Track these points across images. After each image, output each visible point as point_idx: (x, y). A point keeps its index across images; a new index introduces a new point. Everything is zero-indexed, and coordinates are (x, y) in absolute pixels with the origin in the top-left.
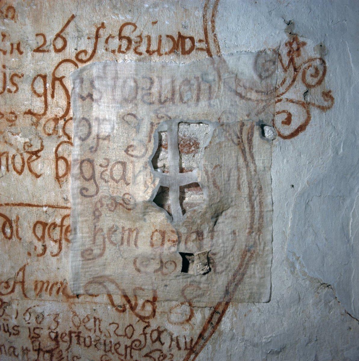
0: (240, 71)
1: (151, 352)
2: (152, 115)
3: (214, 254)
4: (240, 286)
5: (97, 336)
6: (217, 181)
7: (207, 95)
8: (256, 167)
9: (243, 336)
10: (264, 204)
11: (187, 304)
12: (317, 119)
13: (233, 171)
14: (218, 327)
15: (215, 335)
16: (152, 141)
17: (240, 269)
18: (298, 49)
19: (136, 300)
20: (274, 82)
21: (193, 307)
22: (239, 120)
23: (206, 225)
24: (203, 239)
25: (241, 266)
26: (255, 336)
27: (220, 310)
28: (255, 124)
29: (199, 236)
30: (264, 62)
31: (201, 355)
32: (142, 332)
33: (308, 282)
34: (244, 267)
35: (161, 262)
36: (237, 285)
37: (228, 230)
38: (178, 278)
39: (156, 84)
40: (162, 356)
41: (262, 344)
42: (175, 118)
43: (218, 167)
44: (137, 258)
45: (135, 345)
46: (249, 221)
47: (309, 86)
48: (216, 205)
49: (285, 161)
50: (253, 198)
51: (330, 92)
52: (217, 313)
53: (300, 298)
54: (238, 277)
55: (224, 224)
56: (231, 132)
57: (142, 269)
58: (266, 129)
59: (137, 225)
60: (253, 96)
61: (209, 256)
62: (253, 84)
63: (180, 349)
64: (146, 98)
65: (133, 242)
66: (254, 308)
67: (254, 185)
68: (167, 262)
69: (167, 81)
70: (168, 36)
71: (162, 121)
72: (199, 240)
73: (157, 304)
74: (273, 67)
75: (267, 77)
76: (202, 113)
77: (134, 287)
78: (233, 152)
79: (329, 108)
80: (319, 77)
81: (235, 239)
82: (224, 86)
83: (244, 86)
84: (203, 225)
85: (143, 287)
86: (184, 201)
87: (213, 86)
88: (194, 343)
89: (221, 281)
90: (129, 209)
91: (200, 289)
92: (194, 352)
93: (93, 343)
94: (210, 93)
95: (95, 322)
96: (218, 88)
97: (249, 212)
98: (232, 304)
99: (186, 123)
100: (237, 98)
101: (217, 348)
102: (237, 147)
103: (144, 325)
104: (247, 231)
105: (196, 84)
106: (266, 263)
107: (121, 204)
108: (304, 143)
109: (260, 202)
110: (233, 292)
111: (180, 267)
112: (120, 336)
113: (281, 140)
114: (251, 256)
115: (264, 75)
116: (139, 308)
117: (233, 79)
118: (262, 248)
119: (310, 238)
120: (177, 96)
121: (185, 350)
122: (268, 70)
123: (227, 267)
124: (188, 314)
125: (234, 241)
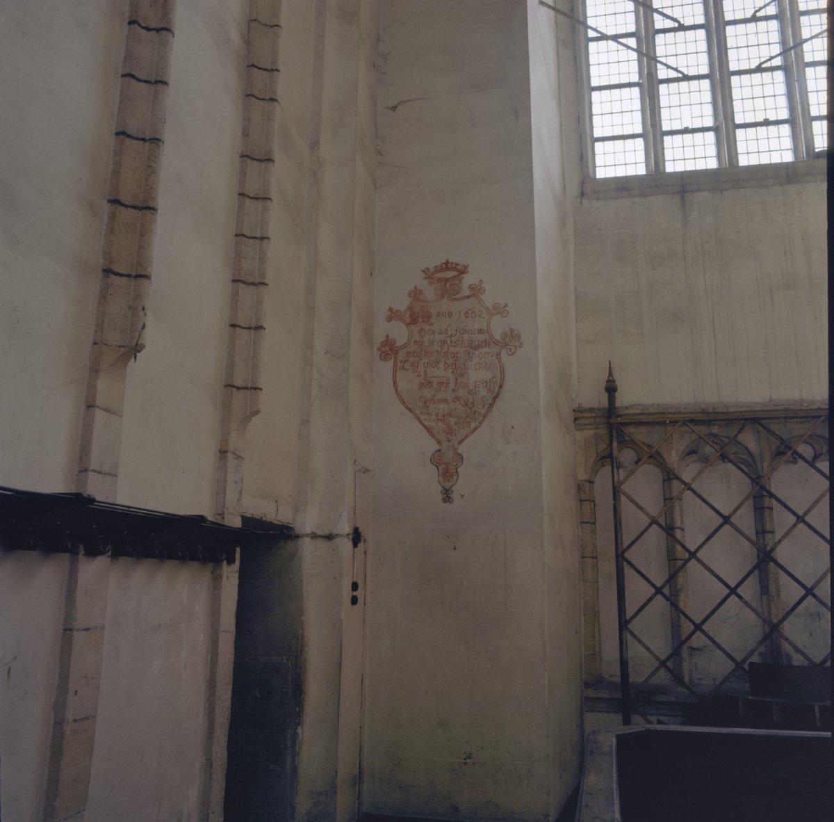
69: (477, 342)
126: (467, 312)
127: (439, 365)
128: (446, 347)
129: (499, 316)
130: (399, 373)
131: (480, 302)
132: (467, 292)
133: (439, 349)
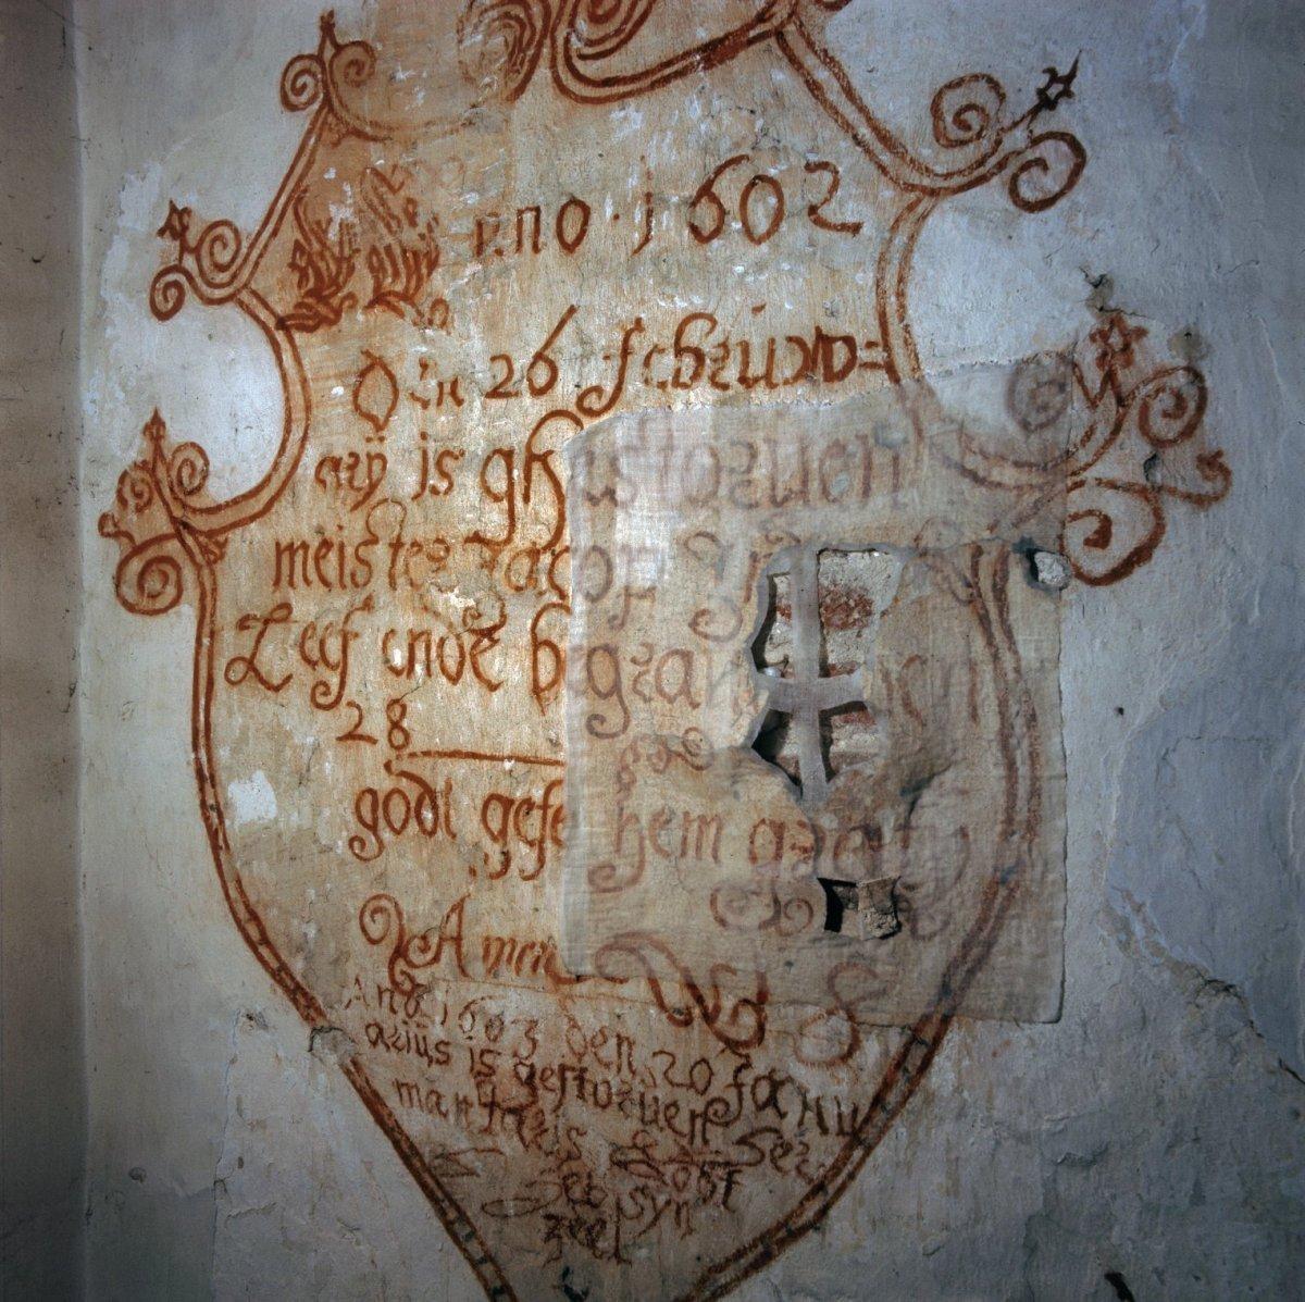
1: (752, 1134)
3: (911, 888)
4: (979, 975)
6: (915, 697)
7: (888, 480)
8: (1018, 660)
10: (1042, 759)
11: (842, 1013)
14: (923, 1081)
15: (916, 1101)
16: (754, 599)
18: (1126, 348)
19: (717, 996)
20: (1062, 437)
21: (859, 1024)
22: (967, 541)
24: (880, 846)
26: (1021, 1113)
27: (928, 1034)
29: (870, 840)
30: (1037, 387)
31: (879, 1151)
32: (730, 1080)
33: (1167, 975)
35: (776, 901)
36: (971, 972)
37: (947, 826)
38: (817, 945)
39: (763, 457)
42: (810, 541)
44: (717, 890)
45: (715, 1114)
46: (1002, 800)
47: (1158, 443)
49: (1098, 642)
50: (1013, 741)
52: (922, 1042)
53: (1144, 1020)
54: (976, 951)
55: (938, 811)
56: (948, 570)
57: (730, 918)
59: (719, 807)
60: (1008, 475)
61: (897, 892)
63: (825, 1131)
65: (709, 851)
66: (1019, 1036)
67: (1014, 709)
68: (790, 902)
69: (788, 449)
70: (790, 339)
71: (777, 549)
72: (872, 848)
73: (768, 1009)
74: (1059, 398)
75: (1042, 426)
76: (876, 525)
77: (710, 963)
79: (1216, 498)
80: (1186, 418)
82: (931, 454)
85: (733, 965)
86: (833, 749)
88: (860, 1119)
89: (931, 958)
90: (699, 768)
91: (875, 976)
92: (861, 1143)
93: (615, 1099)
94: (896, 474)
95: (619, 1045)
96: (916, 461)
98: (959, 1022)
99: (835, 551)
101: (921, 1135)
102: (966, 611)
104: (999, 828)
106: (1050, 917)
107: (680, 755)
109: (1031, 754)
111: (820, 918)
112: (678, 1085)
114: (1010, 898)
116: (724, 1017)
117: (954, 436)
120: (815, 486)
123: (946, 924)
124: (846, 1040)
126: (706, 191)
127: (495, 663)
128: (543, 504)
129: (992, 195)
131: (814, 87)
133: (493, 520)
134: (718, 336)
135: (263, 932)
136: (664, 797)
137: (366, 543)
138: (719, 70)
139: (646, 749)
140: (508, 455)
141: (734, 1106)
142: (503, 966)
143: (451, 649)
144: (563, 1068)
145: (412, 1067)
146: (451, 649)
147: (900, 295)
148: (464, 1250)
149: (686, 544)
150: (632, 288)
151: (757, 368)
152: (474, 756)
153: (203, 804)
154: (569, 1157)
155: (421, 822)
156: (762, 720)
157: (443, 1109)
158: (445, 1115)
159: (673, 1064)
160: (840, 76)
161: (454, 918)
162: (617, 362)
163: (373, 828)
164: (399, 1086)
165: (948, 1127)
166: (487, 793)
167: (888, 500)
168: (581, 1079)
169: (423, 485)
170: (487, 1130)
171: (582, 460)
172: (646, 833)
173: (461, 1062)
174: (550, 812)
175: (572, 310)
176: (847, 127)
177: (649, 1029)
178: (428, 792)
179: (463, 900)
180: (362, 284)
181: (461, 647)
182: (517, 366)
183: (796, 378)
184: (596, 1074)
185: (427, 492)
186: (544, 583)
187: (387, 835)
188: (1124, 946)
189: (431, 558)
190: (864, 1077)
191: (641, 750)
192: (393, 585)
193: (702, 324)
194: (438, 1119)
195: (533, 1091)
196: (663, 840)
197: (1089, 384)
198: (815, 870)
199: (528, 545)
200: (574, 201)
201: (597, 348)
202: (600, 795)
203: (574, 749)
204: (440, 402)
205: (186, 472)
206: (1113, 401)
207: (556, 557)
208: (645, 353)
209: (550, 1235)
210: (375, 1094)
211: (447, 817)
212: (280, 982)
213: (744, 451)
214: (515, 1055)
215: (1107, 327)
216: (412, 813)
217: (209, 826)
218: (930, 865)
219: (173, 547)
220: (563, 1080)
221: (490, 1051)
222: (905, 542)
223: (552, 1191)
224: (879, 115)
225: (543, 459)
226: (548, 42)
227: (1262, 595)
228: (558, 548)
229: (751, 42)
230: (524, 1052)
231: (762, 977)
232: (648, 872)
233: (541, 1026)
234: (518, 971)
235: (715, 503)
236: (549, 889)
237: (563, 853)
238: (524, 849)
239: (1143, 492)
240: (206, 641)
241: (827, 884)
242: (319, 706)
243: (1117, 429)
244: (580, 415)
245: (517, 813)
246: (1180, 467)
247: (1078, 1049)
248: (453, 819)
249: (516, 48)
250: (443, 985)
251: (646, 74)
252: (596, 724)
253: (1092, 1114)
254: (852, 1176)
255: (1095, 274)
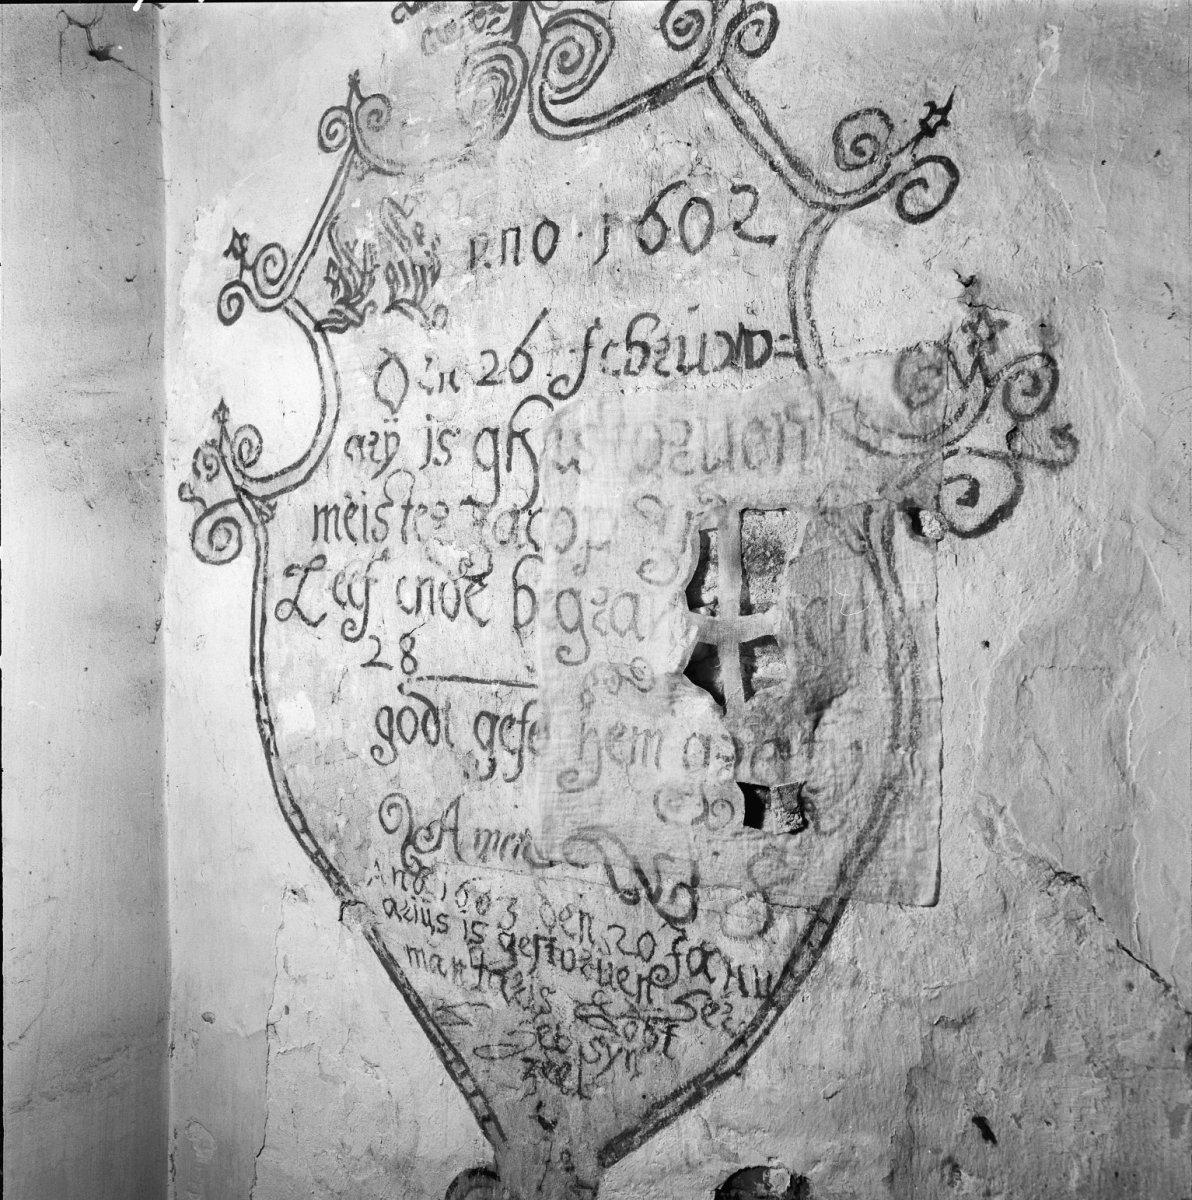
0: (864, 394)
1: (687, 996)
2: (691, 496)
3: (815, 791)
4: (870, 865)
5: (585, 950)
6: (816, 632)
7: (798, 449)
8: (903, 601)
9: (878, 978)
10: (922, 684)
11: (759, 896)
12: (1039, 492)
13: (852, 609)
14: (824, 954)
15: (818, 970)
16: (689, 551)
17: (871, 827)
18: (992, 337)
19: (659, 880)
20: (939, 413)
21: (773, 905)
22: (860, 501)
23: (796, 726)
24: (790, 756)
25: (873, 820)
26: (903, 981)
27: (829, 914)
28: (894, 507)
29: (781, 751)
30: (916, 369)
31: (788, 1011)
32: (670, 951)
33: (1024, 867)
34: (879, 823)
35: (705, 801)
36: (863, 862)
37: (844, 740)
38: (738, 838)
39: (697, 431)
40: (710, 1005)
41: (919, 1001)
42: (733, 502)
43: (819, 603)
44: (659, 792)
45: (658, 978)
46: (889, 720)
47: (1019, 417)
48: (813, 684)
49: (968, 586)
50: (898, 669)
51: (1069, 426)
52: (823, 922)
53: (1005, 903)
54: (867, 846)
55: (836, 727)
56: (844, 525)
57: (669, 815)
58: (925, 516)
59: (661, 723)
60: (896, 445)
61: (803, 795)
62: (892, 421)
63: (745, 994)
64: (677, 462)
65: (653, 759)
66: (903, 916)
67: (899, 642)
68: (716, 802)
69: (717, 425)
70: (718, 334)
71: (707, 508)
72: (782, 757)
73: (699, 892)
74: (937, 381)
75: (923, 404)
76: (787, 487)
77: (654, 852)
78: (852, 570)
79: (1067, 464)
80: (1041, 396)
81: (858, 759)
82: (832, 428)
83: (873, 426)
84: (789, 727)
85: (672, 854)
86: (755, 675)
87: (809, 430)
88: (774, 984)
89: (831, 850)
90: (643, 690)
91: (786, 865)
92: (774, 1005)
93: (579, 964)
94: (804, 445)
95: (581, 920)
96: (820, 434)
97: (887, 700)
98: (853, 904)
99: (755, 510)
100: (860, 453)
101: (823, 998)
102: (859, 559)
103: (674, 935)
104: (887, 742)
105: (775, 429)
106: (929, 818)
107: (628, 679)
108: (1010, 545)
109: (913, 680)
110: (856, 877)
111: (740, 815)
112: (629, 954)
113: (957, 540)
114: (896, 799)
115: (916, 398)
116: (664, 898)
117: (851, 413)
118: (918, 783)
119: (1031, 764)
120: (738, 456)
121: (755, 997)
122: (925, 388)
123: (843, 822)
124: (762, 920)
125: (858, 764)
126: (652, 211)
127: (481, 602)
129: (882, 210)
130: (282, 639)
131: (738, 122)
132: (661, 62)
133: (483, 489)
134: (660, 332)
135: (304, 822)
136: (617, 714)
137: (383, 506)
138: (661, 111)
139: (601, 674)
140: (495, 432)
141: (673, 972)
142: (490, 853)
143: (450, 592)
144: (537, 938)
145: (419, 934)
146: (450, 592)
147: (808, 295)
148: (460, 1085)
149: (635, 505)
150: (592, 293)
151: (692, 358)
152: (468, 680)
153: (259, 717)
154: (542, 1011)
155: (426, 734)
156: (692, 650)
157: (443, 970)
158: (445, 975)
159: (624, 936)
160: (760, 113)
161: (452, 812)
162: (580, 354)
163: (389, 738)
164: (409, 950)
165: (844, 992)
166: (478, 712)
167: (797, 467)
168: (551, 947)
169: (428, 459)
170: (477, 988)
171: (553, 435)
172: (603, 744)
173: (457, 931)
174: (528, 726)
175: (545, 312)
176: (765, 155)
177: (605, 907)
178: (432, 709)
179: (459, 798)
180: (380, 293)
181: (458, 591)
182: (501, 359)
183: (723, 366)
184: (563, 943)
185: (431, 463)
186: (523, 538)
187: (400, 744)
188: (989, 842)
189: (434, 517)
190: (776, 950)
191: (599, 676)
192: (404, 539)
193: (649, 322)
194: (439, 977)
195: (514, 955)
196: (616, 750)
197: (961, 369)
198: (735, 775)
199: (510, 507)
200: (547, 222)
201: (565, 342)
202: (567, 712)
203: (550, 678)
204: (441, 390)
205: (245, 448)
206: (982, 382)
207: (532, 515)
208: (603, 346)
209: (527, 1075)
210: (391, 956)
211: (447, 730)
212: (318, 863)
213: (681, 427)
214: (499, 926)
215: (976, 320)
216: (420, 727)
217: (263, 737)
218: (830, 772)
219: (235, 510)
220: (537, 948)
221: (480, 923)
222: (810, 503)
223: (529, 1039)
224: (790, 144)
225: (522, 435)
226: (526, 90)
227: (1104, 545)
228: (534, 509)
229: (687, 86)
230: (506, 924)
231: (694, 864)
232: (604, 777)
233: (520, 901)
234: (502, 856)
235: (659, 471)
236: (526, 790)
237: (538, 759)
238: (507, 755)
239: (1005, 459)
240: (260, 586)
241: (743, 786)
242: (347, 639)
243: (984, 406)
244: (551, 399)
245: (501, 726)
246: (1037, 433)
247: (951, 928)
248: (451, 731)
249: (502, 95)
250: (443, 868)
251: (604, 115)
252: (563, 654)
253: (962, 984)
254: (767, 1032)
255: (966, 275)
